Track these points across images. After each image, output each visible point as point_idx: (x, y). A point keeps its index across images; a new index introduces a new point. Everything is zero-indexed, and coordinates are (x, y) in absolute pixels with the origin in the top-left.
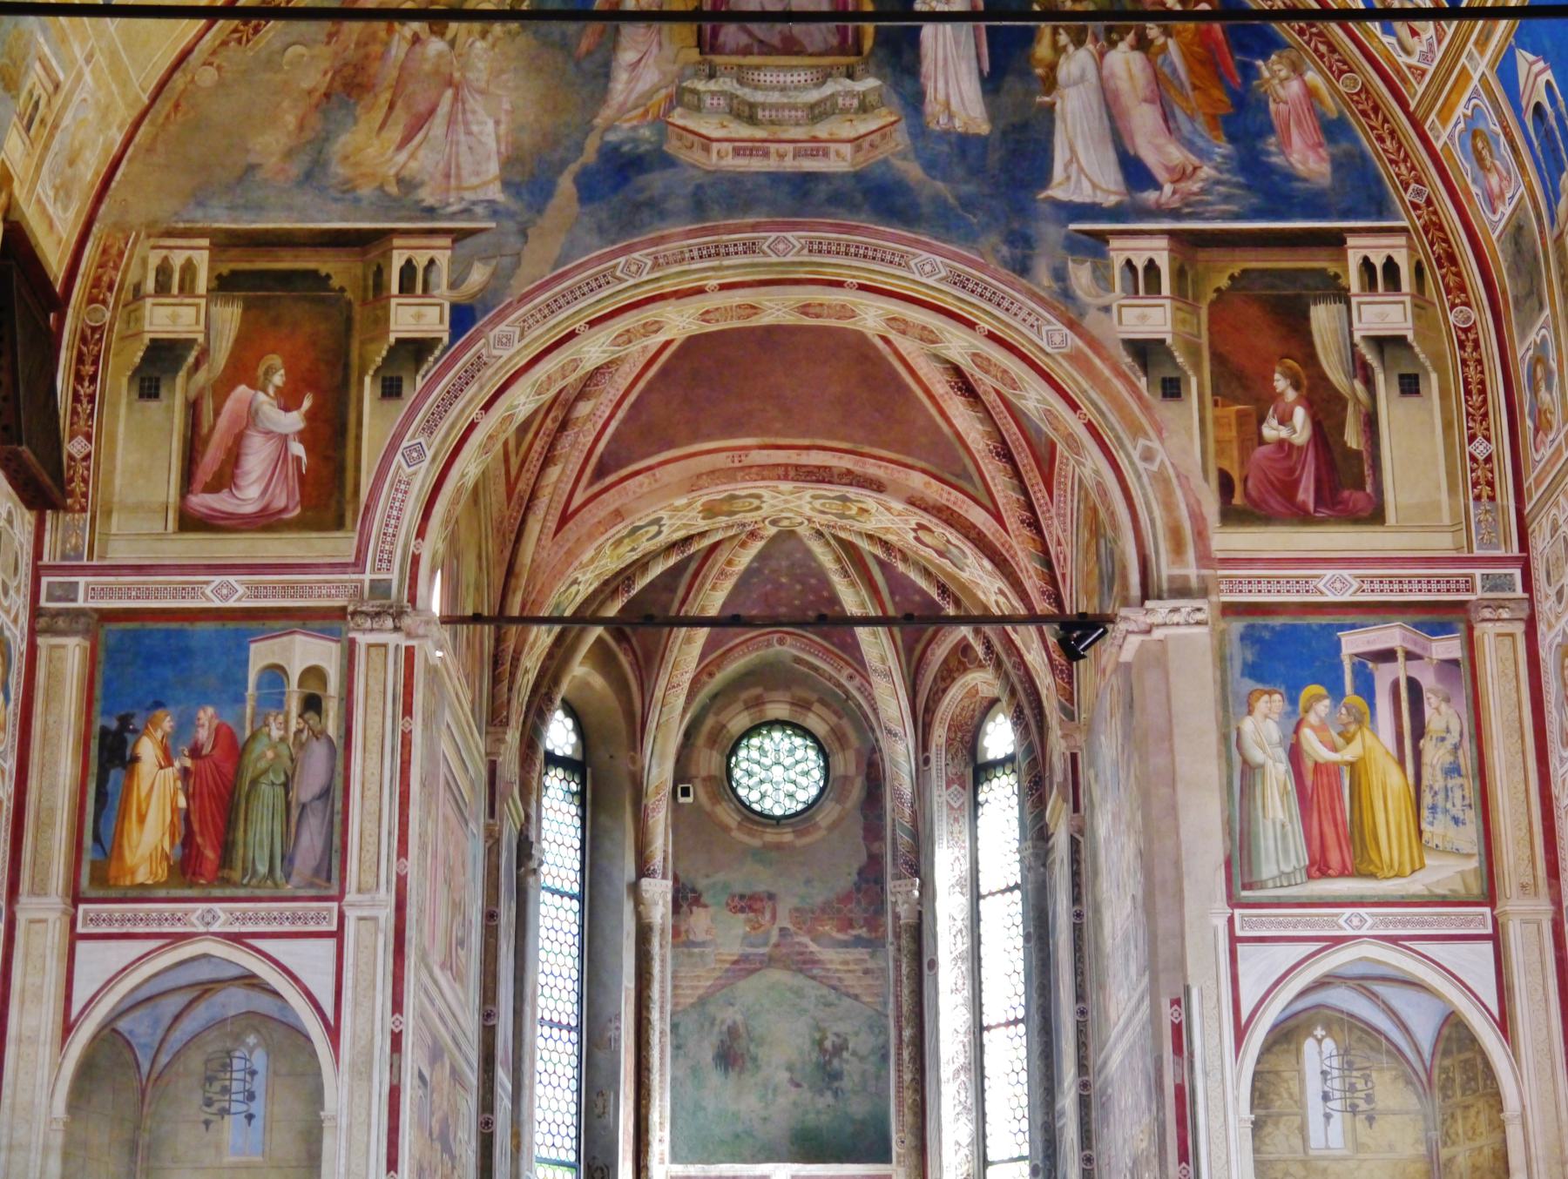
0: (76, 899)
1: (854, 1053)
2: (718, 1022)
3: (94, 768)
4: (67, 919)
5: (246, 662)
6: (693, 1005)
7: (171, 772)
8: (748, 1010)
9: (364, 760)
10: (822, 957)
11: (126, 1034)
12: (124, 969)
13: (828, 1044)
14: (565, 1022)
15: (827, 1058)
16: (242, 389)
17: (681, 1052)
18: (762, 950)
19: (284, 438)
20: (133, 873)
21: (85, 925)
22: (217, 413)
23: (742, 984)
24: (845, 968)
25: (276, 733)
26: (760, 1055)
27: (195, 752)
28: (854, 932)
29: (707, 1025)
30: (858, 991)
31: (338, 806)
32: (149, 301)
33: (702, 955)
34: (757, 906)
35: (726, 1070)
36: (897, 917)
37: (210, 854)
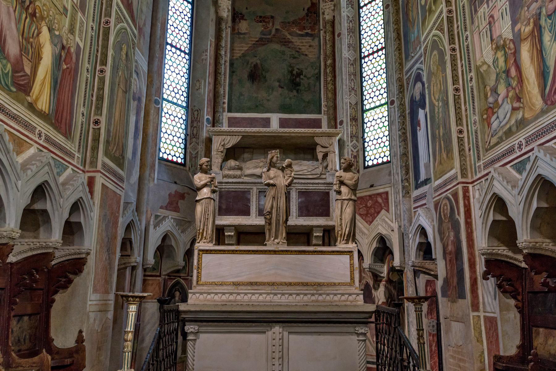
1: (305, 76)
2: (250, 63)
6: (240, 57)
8: (262, 59)
10: (293, 40)
13: (295, 72)
14: (183, 49)
15: (294, 78)
17: (234, 74)
18: (268, 37)
23: (261, 49)
24: (302, 44)
26: (267, 76)
28: (306, 31)
29: (245, 64)
30: (307, 53)
33: (244, 38)
34: (267, 20)
35: (253, 81)
36: (324, 19)
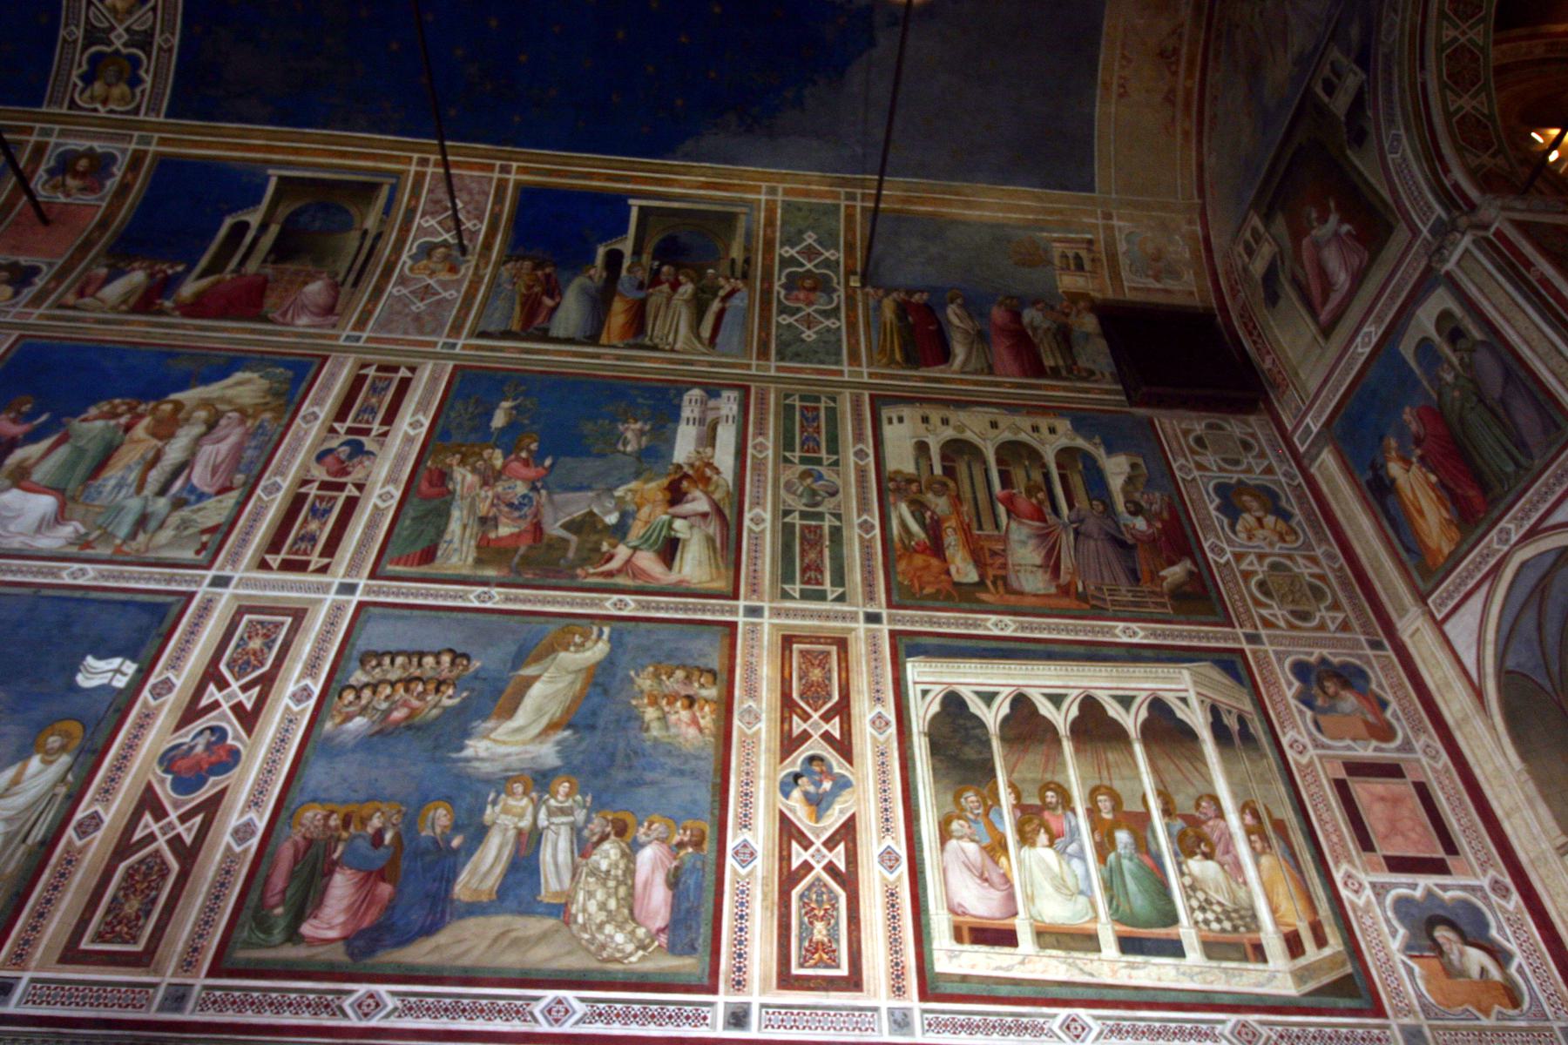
0: (1422, 598)
3: (1378, 509)
4: (1428, 617)
5: (1404, 361)
7: (1414, 468)
9: (1513, 327)
11: (1518, 669)
12: (1482, 621)
16: (1305, 242)
19: (1336, 234)
20: (1440, 550)
21: (1439, 611)
22: (1303, 267)
25: (1449, 378)
27: (1418, 442)
31: (1522, 374)
32: (1251, 267)
37: (1471, 493)
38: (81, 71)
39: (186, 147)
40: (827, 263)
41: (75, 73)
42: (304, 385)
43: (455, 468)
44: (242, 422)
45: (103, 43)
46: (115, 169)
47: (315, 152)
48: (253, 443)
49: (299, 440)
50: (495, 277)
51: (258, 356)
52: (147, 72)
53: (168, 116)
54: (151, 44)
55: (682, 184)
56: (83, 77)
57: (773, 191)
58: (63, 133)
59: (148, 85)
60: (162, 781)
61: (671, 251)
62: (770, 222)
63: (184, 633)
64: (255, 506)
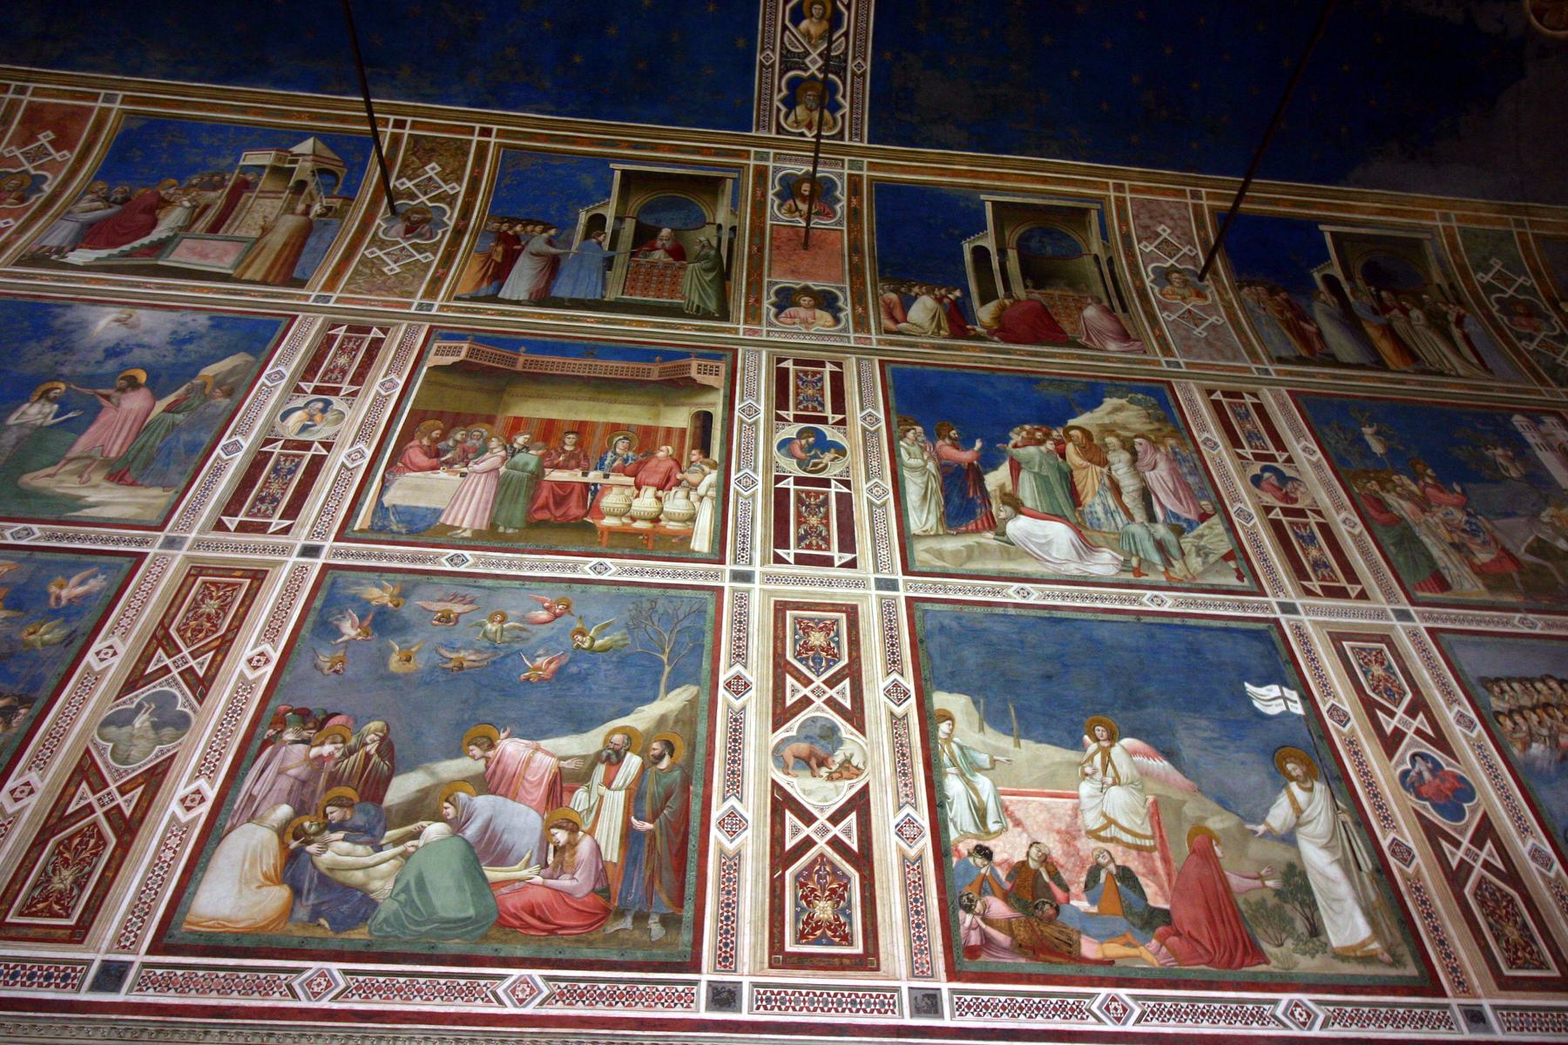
38: (782, 95)
39: (895, 172)
40: (1522, 289)
41: (776, 97)
42: (1175, 411)
43: (1383, 494)
44: (1157, 450)
45: (800, 69)
46: (838, 193)
47: (1018, 178)
48: (1185, 470)
49: (1221, 465)
50: (1242, 302)
51: (1109, 382)
52: (844, 96)
53: (869, 142)
54: (845, 69)
55: (1362, 210)
56: (784, 101)
57: (1445, 217)
58: (777, 157)
59: (847, 110)
60: (1424, 807)
61: (1376, 275)
62: (1454, 248)
63: (1305, 660)
64: (1246, 534)
